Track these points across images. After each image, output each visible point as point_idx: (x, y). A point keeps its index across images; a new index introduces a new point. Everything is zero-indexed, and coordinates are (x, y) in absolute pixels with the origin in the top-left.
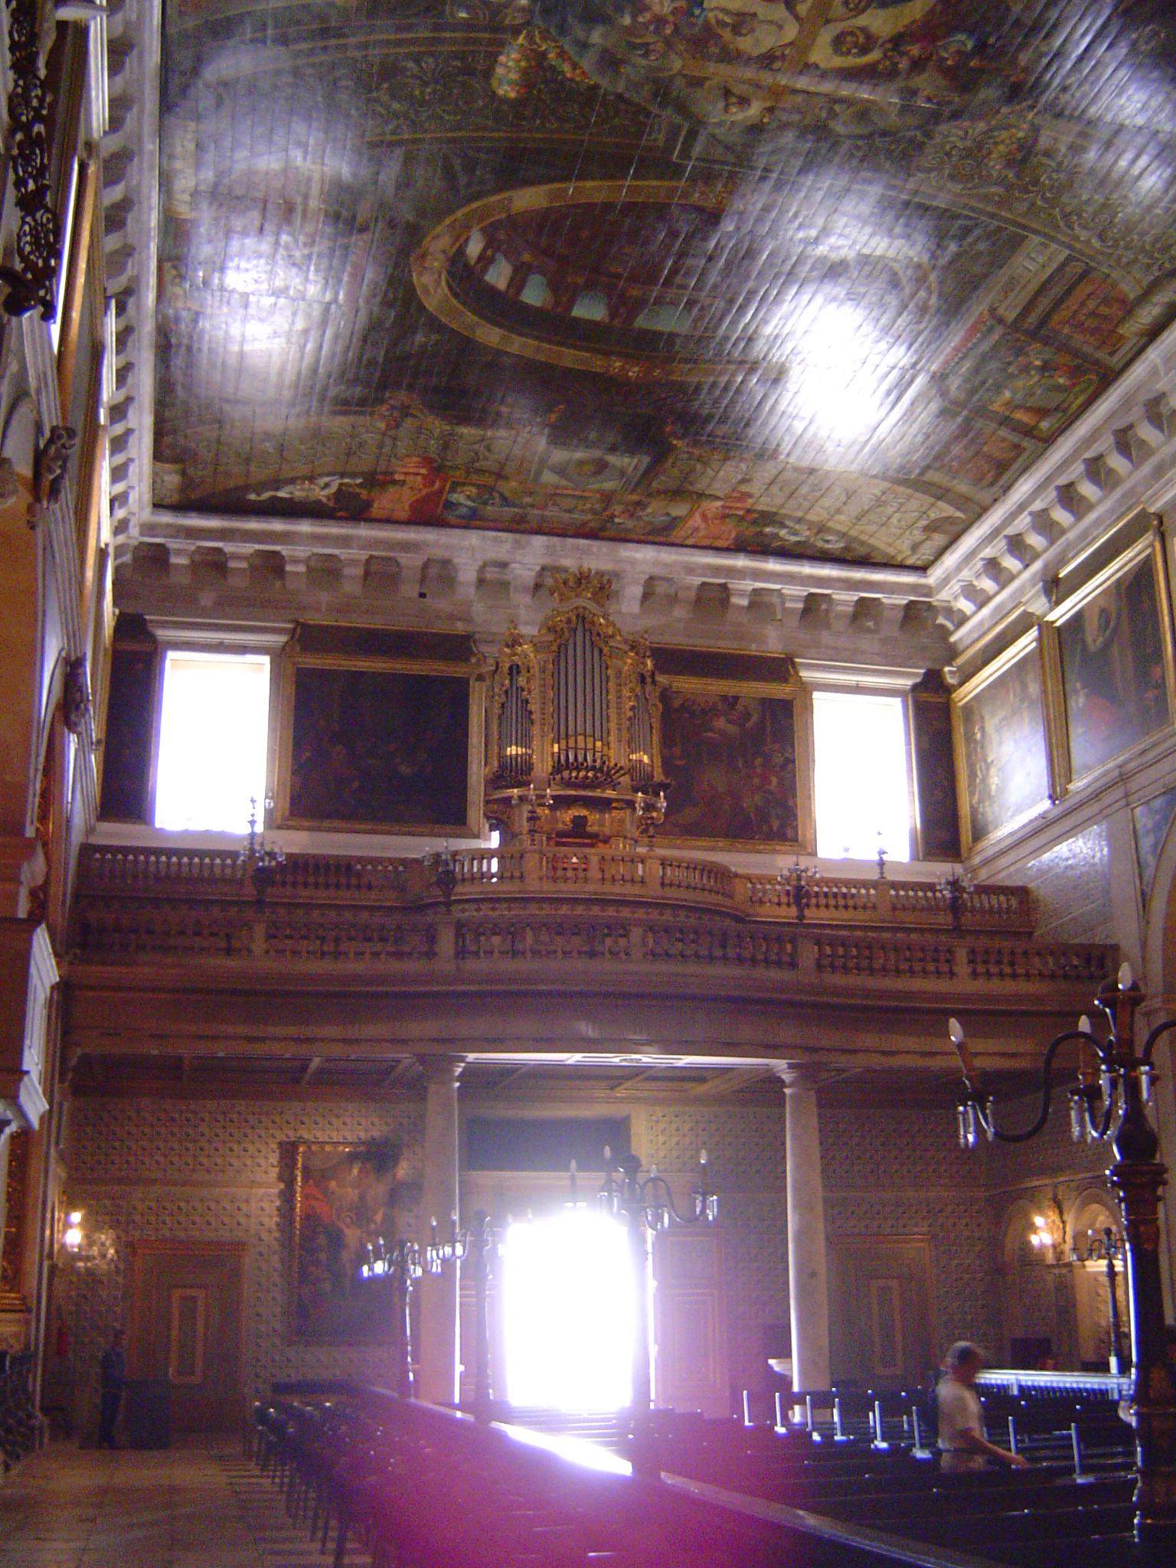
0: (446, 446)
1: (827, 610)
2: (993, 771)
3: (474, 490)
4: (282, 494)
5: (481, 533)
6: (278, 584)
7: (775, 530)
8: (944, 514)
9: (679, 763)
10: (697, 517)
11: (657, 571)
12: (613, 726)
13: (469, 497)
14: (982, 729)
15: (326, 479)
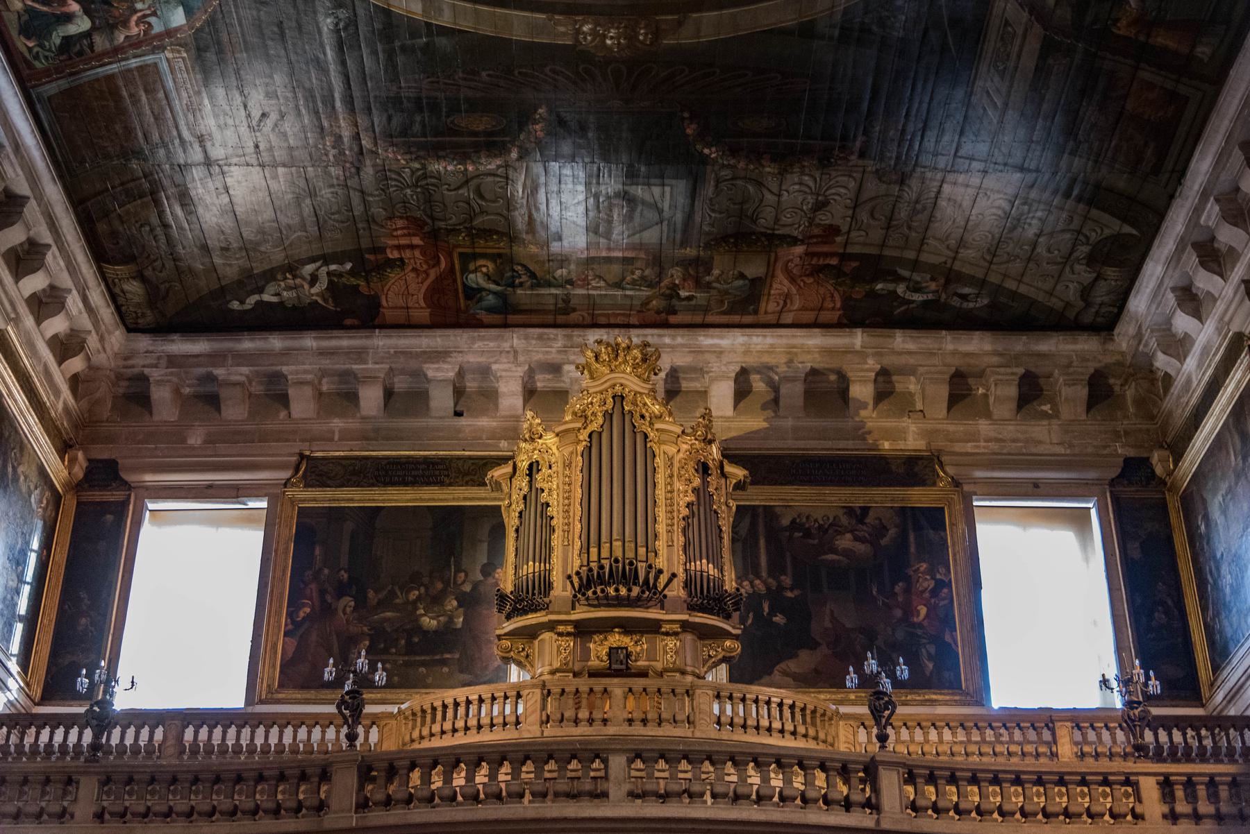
0: (429, 200)
1: (986, 396)
2: (1224, 569)
3: (491, 266)
4: (266, 297)
5: (522, 331)
6: (283, 414)
7: (891, 286)
8: (1107, 232)
9: (789, 594)
10: (780, 276)
11: (751, 361)
12: (661, 528)
13: (488, 277)
14: (1206, 517)
15: (309, 268)
